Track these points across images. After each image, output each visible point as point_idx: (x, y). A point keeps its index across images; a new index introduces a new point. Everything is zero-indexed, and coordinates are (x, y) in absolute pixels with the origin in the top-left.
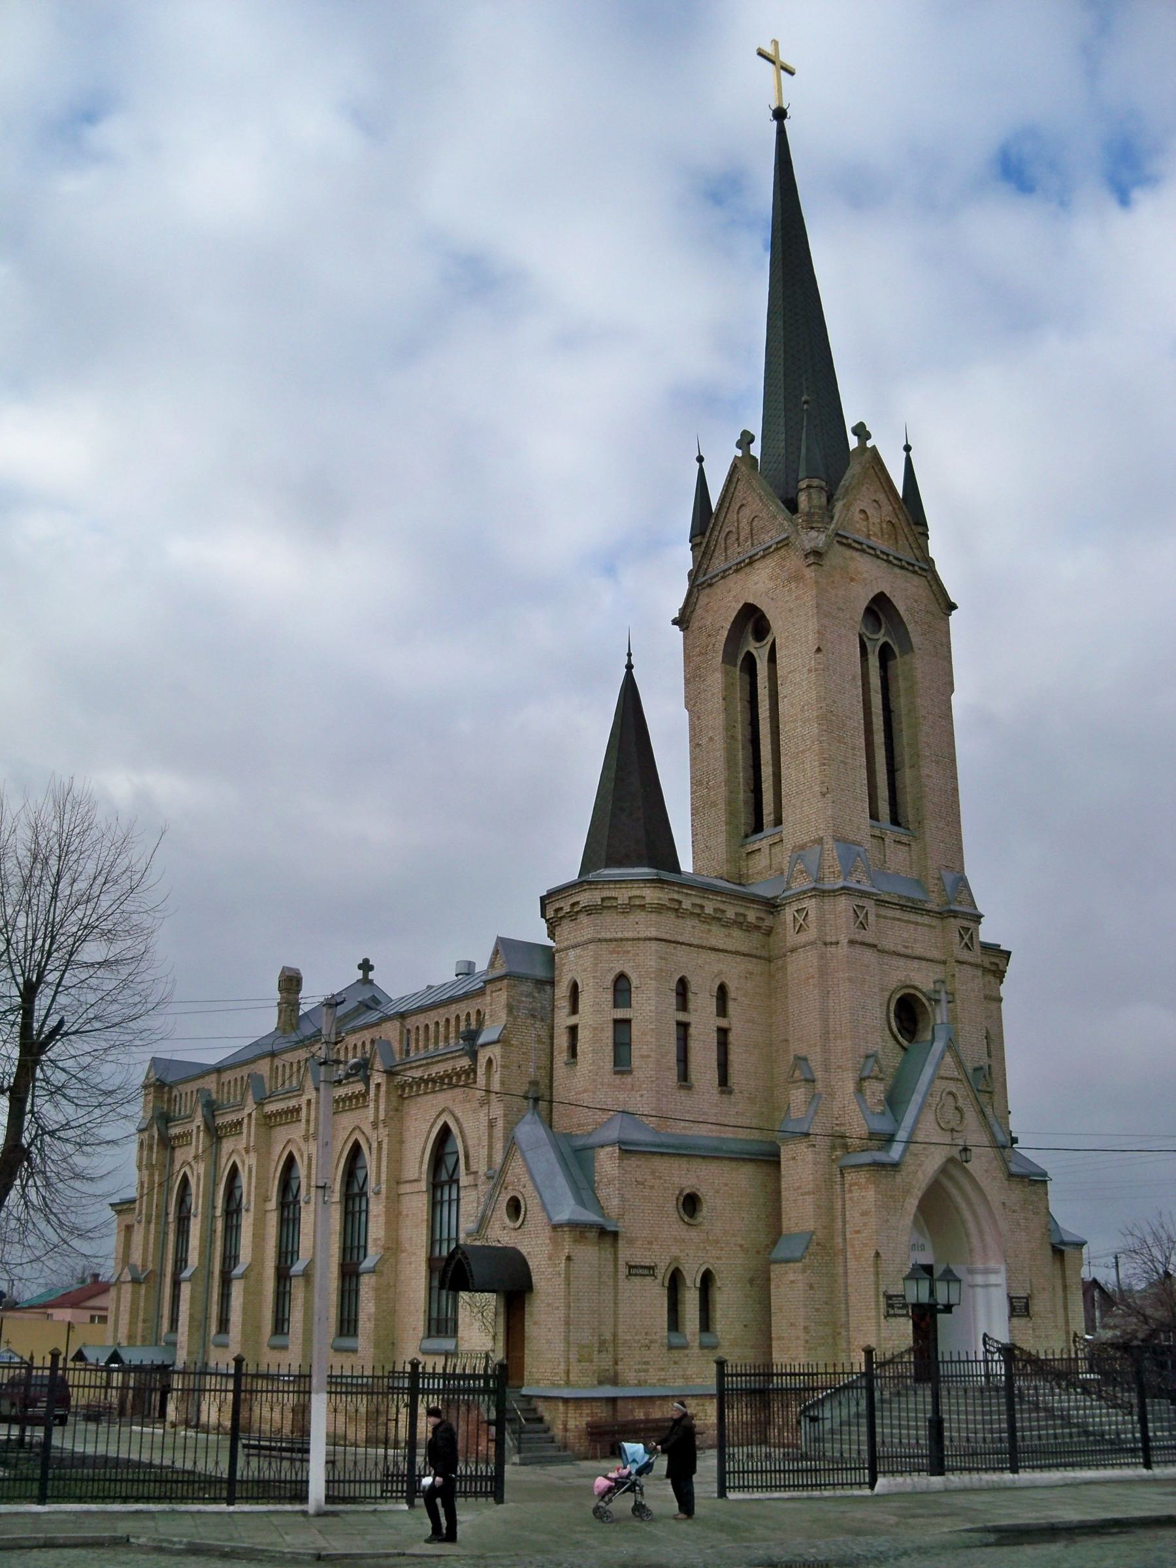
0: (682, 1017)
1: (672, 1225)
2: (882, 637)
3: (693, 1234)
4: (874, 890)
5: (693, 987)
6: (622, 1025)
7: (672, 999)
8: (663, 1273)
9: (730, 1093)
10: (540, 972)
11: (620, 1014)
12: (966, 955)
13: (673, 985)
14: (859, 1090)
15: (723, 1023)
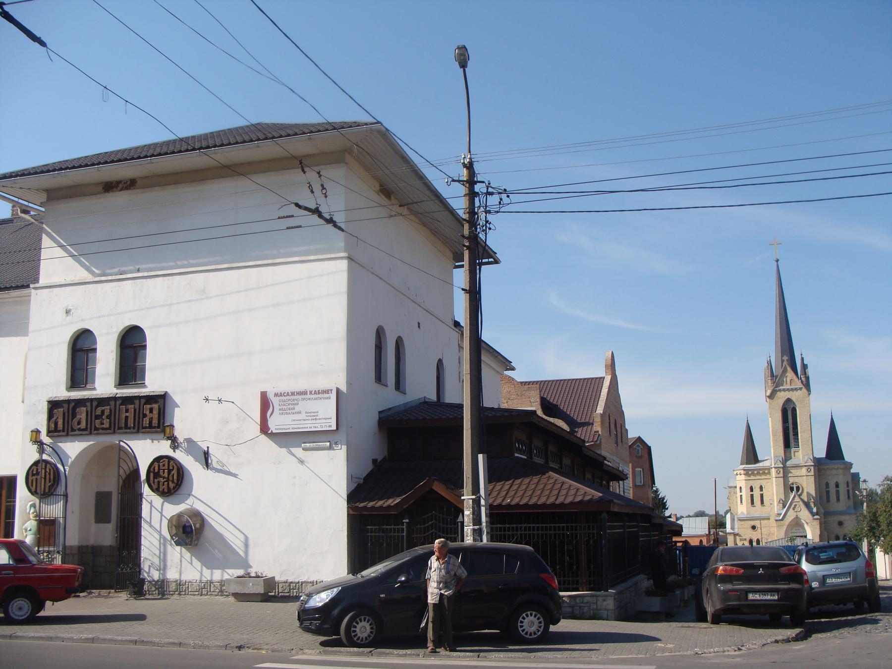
0: (752, 493)
1: (750, 531)
2: (792, 407)
3: (754, 532)
4: (782, 466)
5: (754, 487)
6: (741, 496)
7: (749, 490)
8: (748, 540)
9: (764, 506)
10: (735, 485)
11: (741, 494)
12: (809, 474)
13: (749, 487)
14: (778, 505)
15: (762, 492)
